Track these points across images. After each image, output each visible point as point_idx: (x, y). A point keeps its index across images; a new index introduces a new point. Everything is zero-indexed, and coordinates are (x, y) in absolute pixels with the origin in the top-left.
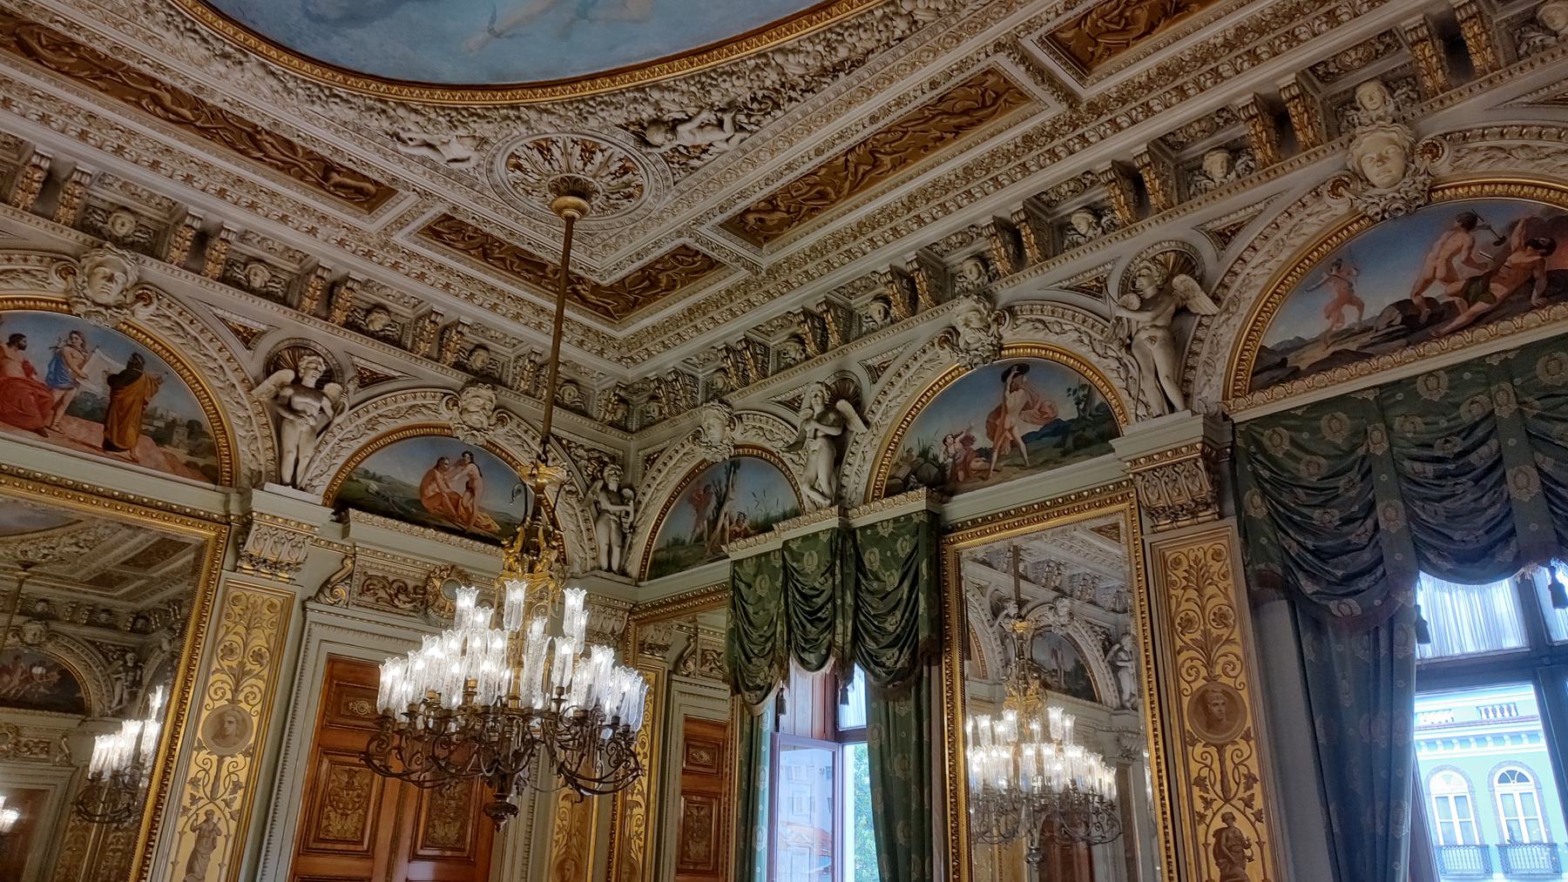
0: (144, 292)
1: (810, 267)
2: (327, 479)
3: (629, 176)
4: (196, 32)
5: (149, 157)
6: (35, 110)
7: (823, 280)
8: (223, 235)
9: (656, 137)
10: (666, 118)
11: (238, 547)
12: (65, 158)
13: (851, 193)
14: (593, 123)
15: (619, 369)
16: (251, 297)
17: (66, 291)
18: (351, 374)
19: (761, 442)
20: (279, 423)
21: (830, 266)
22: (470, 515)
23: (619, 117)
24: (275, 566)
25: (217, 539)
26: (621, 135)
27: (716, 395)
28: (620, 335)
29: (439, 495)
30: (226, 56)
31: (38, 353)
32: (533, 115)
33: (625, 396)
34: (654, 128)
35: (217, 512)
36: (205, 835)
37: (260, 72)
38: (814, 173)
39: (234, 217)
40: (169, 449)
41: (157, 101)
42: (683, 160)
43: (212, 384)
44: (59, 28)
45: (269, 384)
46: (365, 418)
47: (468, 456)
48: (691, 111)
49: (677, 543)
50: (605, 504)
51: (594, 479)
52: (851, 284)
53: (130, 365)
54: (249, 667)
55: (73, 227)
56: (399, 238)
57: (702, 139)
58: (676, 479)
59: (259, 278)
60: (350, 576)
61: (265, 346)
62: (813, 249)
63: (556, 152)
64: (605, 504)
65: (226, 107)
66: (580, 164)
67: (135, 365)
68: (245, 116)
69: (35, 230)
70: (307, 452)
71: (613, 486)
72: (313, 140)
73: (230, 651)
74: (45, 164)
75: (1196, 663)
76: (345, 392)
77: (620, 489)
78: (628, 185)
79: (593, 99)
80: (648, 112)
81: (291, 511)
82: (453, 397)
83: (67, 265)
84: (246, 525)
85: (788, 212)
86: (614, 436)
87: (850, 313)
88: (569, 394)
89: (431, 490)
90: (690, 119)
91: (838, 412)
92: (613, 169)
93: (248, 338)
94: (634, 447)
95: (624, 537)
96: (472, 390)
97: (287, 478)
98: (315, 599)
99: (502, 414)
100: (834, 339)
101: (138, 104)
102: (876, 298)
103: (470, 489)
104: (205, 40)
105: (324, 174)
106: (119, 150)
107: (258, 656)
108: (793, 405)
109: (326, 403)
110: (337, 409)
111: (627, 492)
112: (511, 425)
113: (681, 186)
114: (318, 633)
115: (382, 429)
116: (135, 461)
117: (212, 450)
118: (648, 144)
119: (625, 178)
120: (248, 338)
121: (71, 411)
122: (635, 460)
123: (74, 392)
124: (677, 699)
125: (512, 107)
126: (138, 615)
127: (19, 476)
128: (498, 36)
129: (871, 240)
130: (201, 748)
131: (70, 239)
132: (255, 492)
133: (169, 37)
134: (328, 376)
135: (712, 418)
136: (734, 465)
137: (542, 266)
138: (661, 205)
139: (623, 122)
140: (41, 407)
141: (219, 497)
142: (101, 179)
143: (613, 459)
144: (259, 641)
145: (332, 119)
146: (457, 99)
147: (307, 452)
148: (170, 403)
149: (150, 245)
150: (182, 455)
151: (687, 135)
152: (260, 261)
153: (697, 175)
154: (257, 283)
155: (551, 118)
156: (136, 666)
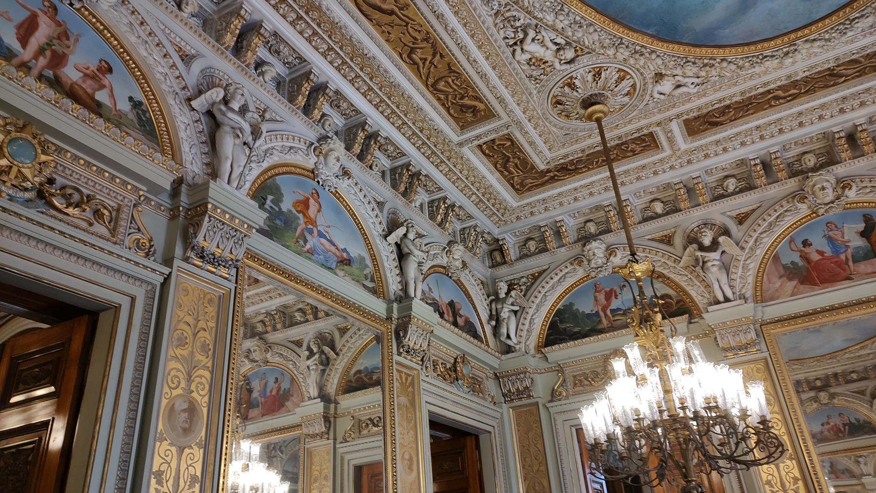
0: (843, 184)
4: (766, 57)
5: (795, 123)
6: (736, 143)
8: (859, 129)
12: (763, 152)
16: (534, 258)
17: (809, 208)
30: (787, 54)
31: (819, 242)
37: (808, 45)
41: (777, 98)
44: (717, 106)
53: (866, 222)
55: (790, 178)
65: (807, 73)
68: (820, 69)
69: (774, 191)
72: (863, 49)
74: (758, 161)
75: (179, 374)
83: (800, 196)
101: (771, 106)
104: (773, 56)
106: (781, 131)
121: (855, 261)
123: (850, 251)
127: (855, 304)
131: (792, 184)
133: (757, 69)
140: (840, 266)
145: (863, 31)
149: (829, 159)
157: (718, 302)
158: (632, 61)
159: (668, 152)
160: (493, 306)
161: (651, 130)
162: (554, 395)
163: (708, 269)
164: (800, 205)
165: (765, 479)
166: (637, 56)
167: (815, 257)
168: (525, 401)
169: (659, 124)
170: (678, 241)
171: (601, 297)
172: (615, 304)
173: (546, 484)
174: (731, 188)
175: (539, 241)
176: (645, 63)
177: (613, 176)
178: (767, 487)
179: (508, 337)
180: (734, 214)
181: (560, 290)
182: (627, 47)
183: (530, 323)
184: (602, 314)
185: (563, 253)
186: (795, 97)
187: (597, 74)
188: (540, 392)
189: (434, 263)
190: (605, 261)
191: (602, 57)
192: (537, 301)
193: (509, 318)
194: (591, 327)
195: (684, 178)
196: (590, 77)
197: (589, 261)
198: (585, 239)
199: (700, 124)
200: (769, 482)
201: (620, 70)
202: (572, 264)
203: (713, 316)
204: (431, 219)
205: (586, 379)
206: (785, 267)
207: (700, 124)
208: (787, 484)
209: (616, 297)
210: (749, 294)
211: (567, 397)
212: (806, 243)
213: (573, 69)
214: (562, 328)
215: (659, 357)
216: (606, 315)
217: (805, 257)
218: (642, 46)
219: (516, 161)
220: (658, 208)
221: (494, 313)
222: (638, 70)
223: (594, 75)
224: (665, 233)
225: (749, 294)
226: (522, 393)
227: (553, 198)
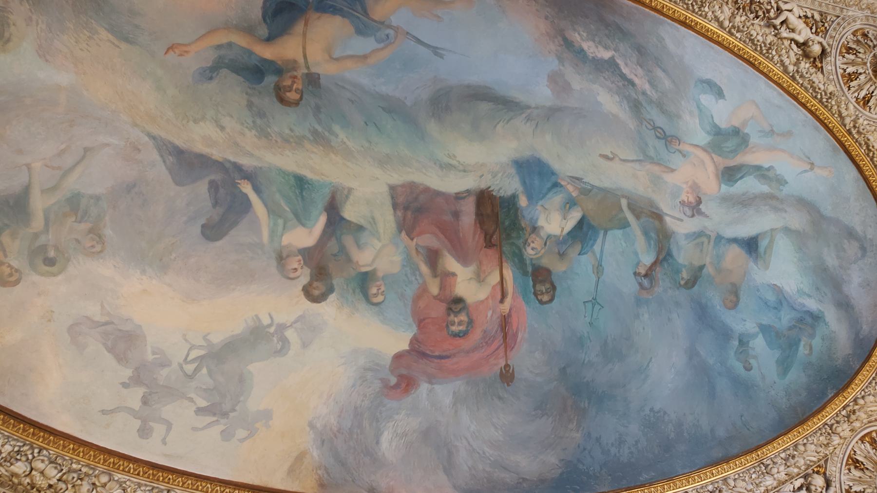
3: (852, 45)
9: (816, 49)
10: (800, 53)
14: (831, 88)
23: (818, 78)
26: (828, 67)
32: (848, 121)
34: (812, 55)
42: (820, 24)
48: (787, 43)
57: (800, 25)
63: (863, 94)
66: (862, 77)
78: (858, 42)
79: (816, 97)
80: (805, 65)
90: (792, 40)
92: (852, 57)
113: (838, 12)
118: (824, 51)
119: (854, 46)
125: (849, 132)
128: (812, 164)
138: (859, 14)
139: (819, 73)
151: (804, 33)
153: (824, 9)
155: (843, 111)
158: (857, 424)
166: (853, 417)
176: (866, 413)
182: (838, 422)
187: (856, 464)
191: (837, 451)
196: (857, 473)
201: (862, 439)
213: (838, 486)
218: (844, 408)
222: (870, 422)
223: (856, 467)
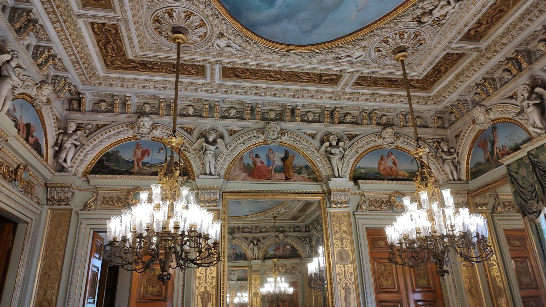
0: (283, 132)
1: (504, 41)
2: (348, 173)
3: (419, 37)
4: (275, 52)
5: (273, 93)
6: (243, 91)
7: (511, 44)
8: (298, 108)
9: (425, 19)
10: (427, 11)
11: (329, 199)
12: (254, 102)
13: (514, 4)
14: (400, 25)
15: (434, 107)
17: (264, 138)
18: (345, 137)
19: (503, 116)
20: (329, 159)
21: (513, 37)
22: (397, 173)
23: (409, 18)
24: (341, 203)
25: (323, 198)
26: (412, 24)
27: (478, 104)
28: (431, 94)
29: (385, 169)
30: (284, 55)
31: (263, 158)
32: (379, 31)
33: (440, 116)
34: (423, 16)
35: (320, 190)
36: (347, 290)
37: (294, 56)
38: (495, 4)
39: (299, 102)
40: (302, 175)
41: (270, 76)
42: (438, 23)
43: (308, 153)
44: (243, 67)
45: (323, 148)
46: (354, 151)
47: (390, 153)
48: (436, 4)
49: (479, 164)
50: (445, 157)
51: (438, 149)
52: (526, 40)
53: (285, 154)
54: (343, 236)
56: (347, 90)
57: (443, 12)
58: (470, 140)
59: (311, 117)
60: (365, 202)
61: (318, 137)
62: (503, 33)
63: (390, 40)
64: (445, 157)
65: (288, 70)
66: (400, 41)
67: (287, 153)
68: (294, 70)
69: (253, 124)
70: (340, 166)
71: (446, 149)
72: (314, 69)
73: (337, 232)
74: (250, 105)
76: (345, 144)
77: (449, 150)
78: (419, 41)
79: (398, 16)
80: (419, 12)
81: (341, 184)
82: (379, 135)
83: (262, 131)
84: (330, 192)
85: (487, 23)
86: (440, 131)
87: (529, 52)
88: (419, 121)
89: (382, 168)
90: (436, 7)
91: (536, 93)
92: (412, 37)
93: (313, 136)
94: (449, 133)
95: (456, 167)
96: (385, 131)
97: (337, 175)
98: (356, 211)
99: (397, 136)
100: (524, 65)
101: (266, 79)
102: (540, 41)
103: (394, 164)
104: (278, 53)
105: (321, 78)
106: (265, 94)
107: (345, 232)
108: (514, 97)
109: (341, 149)
110: (345, 150)
111: (452, 150)
112: (402, 138)
113: (440, 32)
114: (361, 222)
115: (360, 152)
116: (294, 181)
117: (313, 172)
118: (423, 23)
119: (418, 39)
120: (313, 136)
122: (451, 137)
123: (274, 166)
124: (498, 223)
125: (371, 32)
126: (306, 226)
127: (268, 193)
128: (360, 11)
129: (530, 19)
130: (337, 263)
131: (261, 124)
132: (329, 182)
133: (269, 57)
134: (339, 141)
135: (479, 114)
136: (494, 128)
137: (396, 81)
138: (434, 43)
139: (411, 20)
140: (268, 172)
141: (320, 186)
142: (263, 104)
143: (443, 140)
144: (344, 228)
145: (318, 61)
146: (353, 38)
147: (340, 166)
148: (299, 162)
149: (280, 119)
150: (306, 176)
151: (436, 13)
152: (309, 112)
153: (445, 26)
154: (311, 119)
155: (386, 30)
156: (310, 242)
157: (206, 174)
158: (211, 18)
159: (208, 81)
160: (61, 137)
161: (204, 64)
162: (86, 207)
163: (207, 154)
164: (261, 136)
165: (337, 272)
166: (215, 17)
167: (259, 164)
168: (62, 207)
169: (210, 62)
170: (196, 133)
171: (139, 153)
172: (146, 159)
173: (60, 263)
174: (232, 115)
175: (110, 104)
176: (217, 24)
177: (177, 82)
178: (197, 280)
179: (65, 161)
180: (229, 129)
181: (113, 140)
182: (212, 9)
183: (85, 156)
184: (136, 163)
185: (123, 118)
186: (279, 79)
187: (188, 16)
188: (77, 202)
189: (24, 91)
190: (149, 131)
191: (195, 6)
192: (95, 143)
193: (70, 148)
194: (126, 169)
195: (211, 99)
196: (183, 15)
197: (139, 128)
198: (141, 114)
199: (231, 73)
200: (339, 274)
201: (202, 20)
202: (127, 126)
203: (201, 181)
204: (33, 58)
205: (112, 201)
206: (244, 165)
207: (231, 73)
208: (208, 279)
209: (148, 155)
210: (222, 174)
211: (95, 210)
212: (257, 156)
213: (175, 5)
214: (106, 165)
215: (171, 196)
216: (138, 164)
217: (254, 163)
218: (220, 13)
219: (114, 45)
220: (191, 111)
221: (59, 142)
222: (212, 25)
223: (186, 16)
224: (190, 126)
225: (222, 174)
226: (63, 201)
227: (130, 80)
